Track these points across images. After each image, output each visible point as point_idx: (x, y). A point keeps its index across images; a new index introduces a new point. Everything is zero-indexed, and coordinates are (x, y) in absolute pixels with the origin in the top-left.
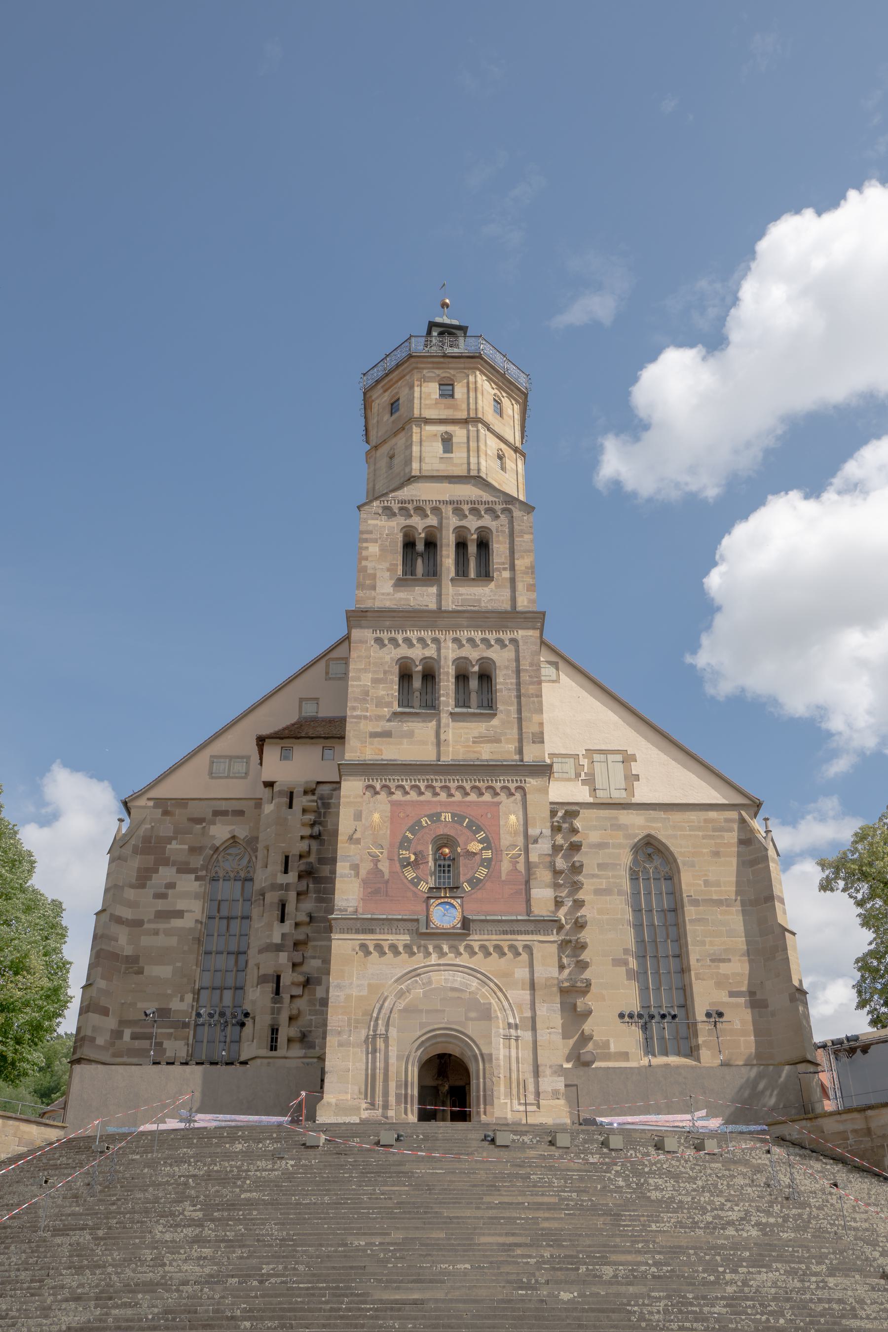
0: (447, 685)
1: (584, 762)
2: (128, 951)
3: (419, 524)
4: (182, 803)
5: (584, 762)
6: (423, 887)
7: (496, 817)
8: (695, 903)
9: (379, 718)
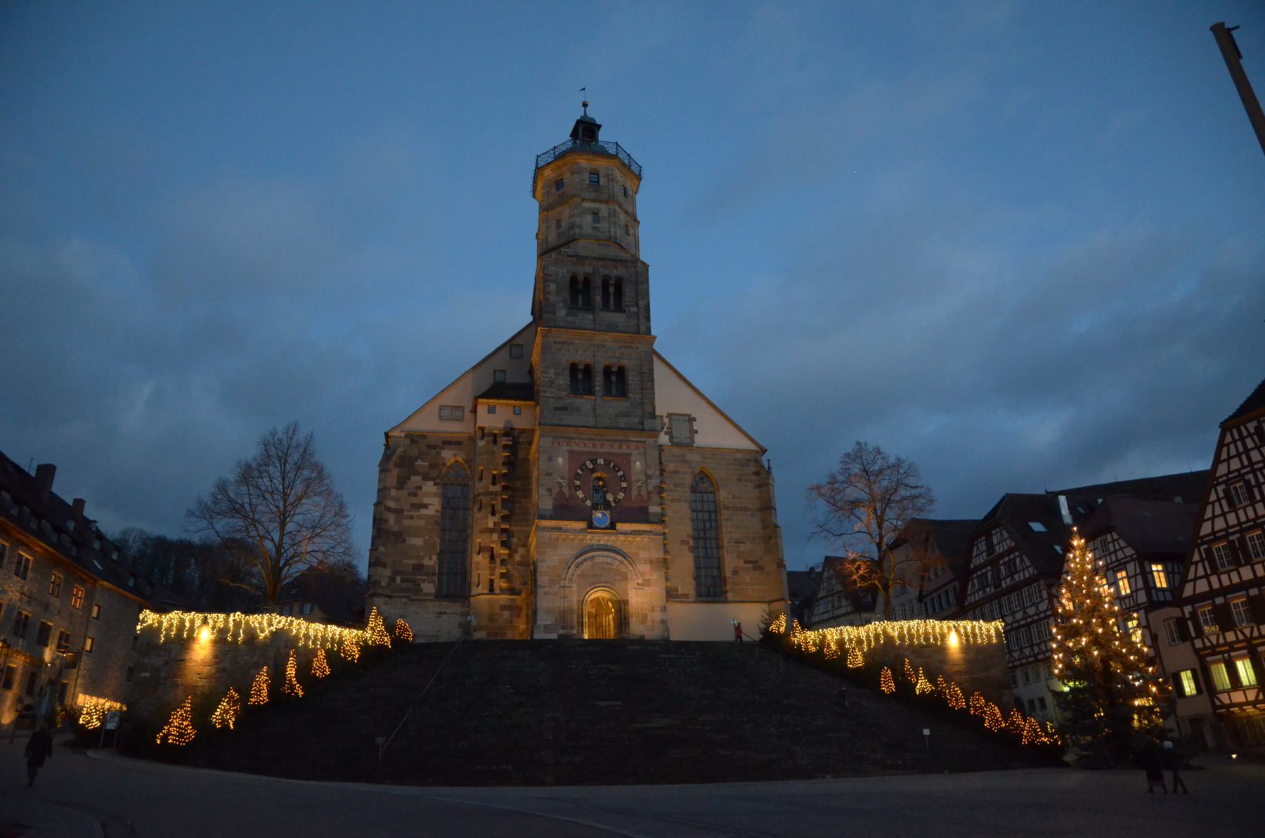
0: (599, 380)
1: (666, 420)
2: (395, 528)
3: (582, 270)
4: (423, 436)
5: (666, 420)
6: (589, 503)
7: (629, 462)
8: (727, 508)
9: (561, 398)
